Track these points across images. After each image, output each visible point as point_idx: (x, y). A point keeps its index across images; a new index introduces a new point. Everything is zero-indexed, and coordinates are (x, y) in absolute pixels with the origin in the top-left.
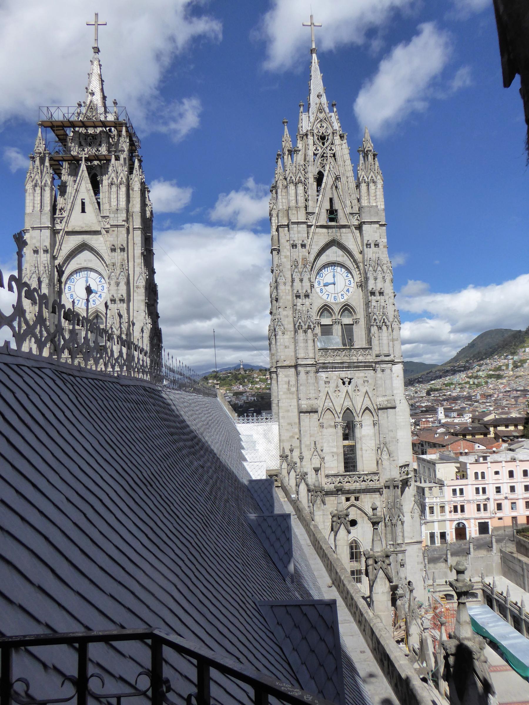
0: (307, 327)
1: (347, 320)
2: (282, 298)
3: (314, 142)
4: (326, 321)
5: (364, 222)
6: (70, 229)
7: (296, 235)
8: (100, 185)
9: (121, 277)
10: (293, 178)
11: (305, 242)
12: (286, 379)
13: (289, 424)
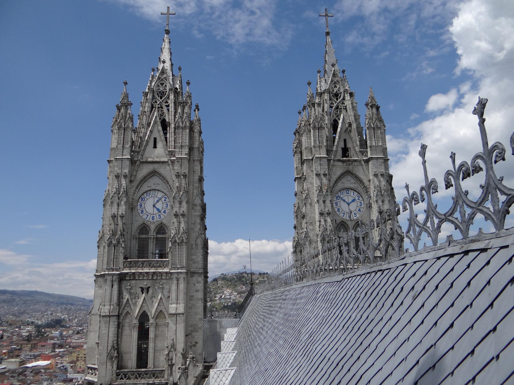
5: (372, 158)
6: (144, 160)
7: (319, 167)
8: (168, 128)
9: (183, 197)
10: (317, 124)
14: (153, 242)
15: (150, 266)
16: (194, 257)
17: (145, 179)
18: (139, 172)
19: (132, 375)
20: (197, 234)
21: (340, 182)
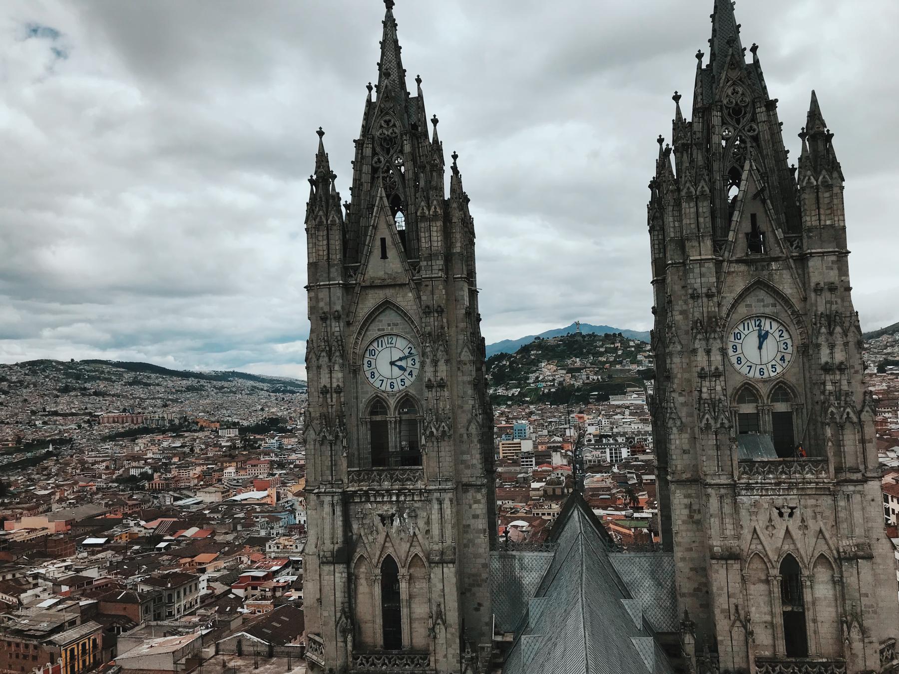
0: (719, 426)
1: (781, 407)
2: (676, 377)
3: (722, 120)
4: (748, 408)
5: (811, 253)
6: (368, 283)
7: (698, 280)
10: (692, 189)
12: (687, 501)
13: (691, 569)
14: (395, 428)
15: (392, 478)
16: (466, 457)
17: (371, 317)
18: (360, 306)
19: (379, 659)
20: (470, 416)
21: (743, 305)
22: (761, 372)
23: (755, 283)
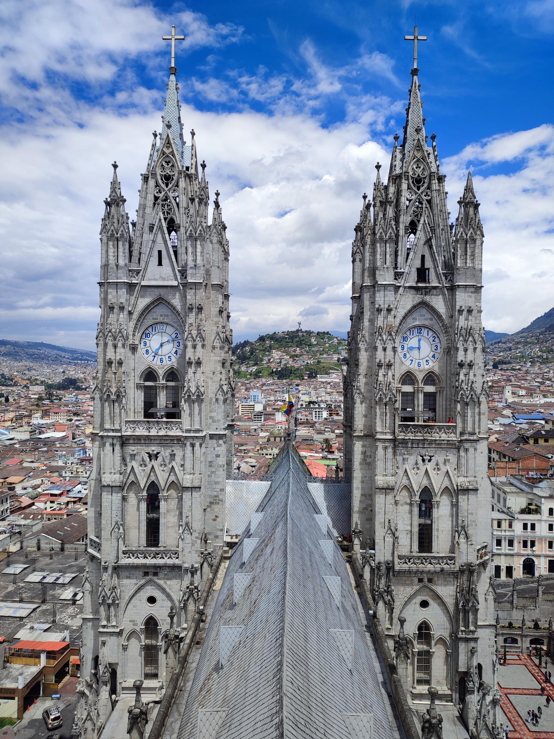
0: (388, 399)
1: (430, 389)
4: (408, 389)
5: (458, 285)
11: (392, 306)
17: (147, 309)
22: (419, 365)
23: (420, 303)
